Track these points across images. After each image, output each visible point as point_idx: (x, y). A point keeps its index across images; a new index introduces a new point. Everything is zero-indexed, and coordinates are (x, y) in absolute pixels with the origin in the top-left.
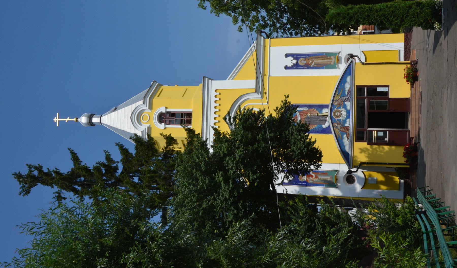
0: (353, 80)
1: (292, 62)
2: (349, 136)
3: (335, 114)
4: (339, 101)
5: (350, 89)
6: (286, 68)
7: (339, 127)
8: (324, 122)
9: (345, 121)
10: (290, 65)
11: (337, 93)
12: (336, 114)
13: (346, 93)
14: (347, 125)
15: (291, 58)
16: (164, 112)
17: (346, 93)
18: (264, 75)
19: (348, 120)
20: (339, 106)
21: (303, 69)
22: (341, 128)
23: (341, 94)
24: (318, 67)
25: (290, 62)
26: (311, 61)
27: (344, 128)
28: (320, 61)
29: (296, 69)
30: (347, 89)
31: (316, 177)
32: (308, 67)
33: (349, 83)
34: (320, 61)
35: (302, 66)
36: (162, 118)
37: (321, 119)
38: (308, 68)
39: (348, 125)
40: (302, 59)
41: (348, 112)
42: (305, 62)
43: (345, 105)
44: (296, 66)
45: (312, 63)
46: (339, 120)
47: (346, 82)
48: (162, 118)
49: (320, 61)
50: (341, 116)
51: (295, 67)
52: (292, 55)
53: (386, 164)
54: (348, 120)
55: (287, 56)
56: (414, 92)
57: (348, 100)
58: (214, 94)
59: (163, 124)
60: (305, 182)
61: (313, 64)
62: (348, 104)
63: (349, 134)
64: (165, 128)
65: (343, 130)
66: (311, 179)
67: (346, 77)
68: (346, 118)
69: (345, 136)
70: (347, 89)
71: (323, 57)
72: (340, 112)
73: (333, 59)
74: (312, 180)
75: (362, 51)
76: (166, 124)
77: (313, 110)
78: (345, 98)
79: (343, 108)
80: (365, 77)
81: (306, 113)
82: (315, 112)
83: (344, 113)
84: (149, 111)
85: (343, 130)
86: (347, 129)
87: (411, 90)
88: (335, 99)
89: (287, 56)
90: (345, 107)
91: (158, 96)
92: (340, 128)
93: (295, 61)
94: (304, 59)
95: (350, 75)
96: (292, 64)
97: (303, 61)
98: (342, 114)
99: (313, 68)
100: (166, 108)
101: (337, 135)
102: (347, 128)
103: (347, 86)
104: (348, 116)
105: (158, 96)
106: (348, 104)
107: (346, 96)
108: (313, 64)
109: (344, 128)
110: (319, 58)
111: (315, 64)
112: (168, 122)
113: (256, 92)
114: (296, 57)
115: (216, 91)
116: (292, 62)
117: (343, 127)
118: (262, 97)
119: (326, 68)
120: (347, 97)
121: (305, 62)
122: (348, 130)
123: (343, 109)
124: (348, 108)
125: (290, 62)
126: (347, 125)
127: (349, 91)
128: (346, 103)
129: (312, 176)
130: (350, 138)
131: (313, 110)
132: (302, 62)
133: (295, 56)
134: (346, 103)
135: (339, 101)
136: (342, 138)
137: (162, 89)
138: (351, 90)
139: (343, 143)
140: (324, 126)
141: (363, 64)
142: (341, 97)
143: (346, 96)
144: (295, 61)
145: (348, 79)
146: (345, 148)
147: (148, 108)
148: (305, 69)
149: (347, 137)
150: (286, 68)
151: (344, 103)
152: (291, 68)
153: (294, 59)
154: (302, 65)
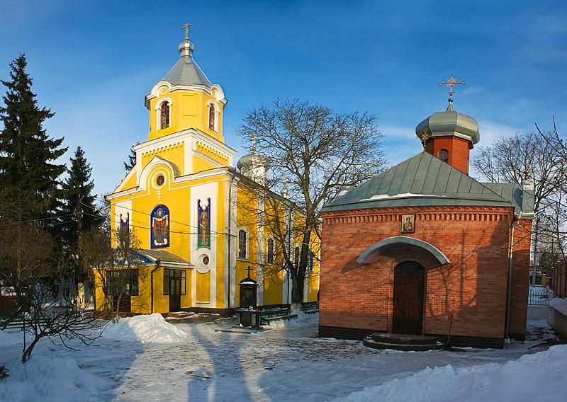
6: (199, 201)
15: (207, 203)
25: (204, 205)
32: (200, 221)
36: (165, 104)
38: (199, 221)
44: (200, 210)
52: (209, 205)
55: (209, 200)
82: (165, 233)
89: (209, 200)
93: (204, 208)
125: (204, 205)
140: (155, 241)
144: (204, 208)
150: (199, 201)
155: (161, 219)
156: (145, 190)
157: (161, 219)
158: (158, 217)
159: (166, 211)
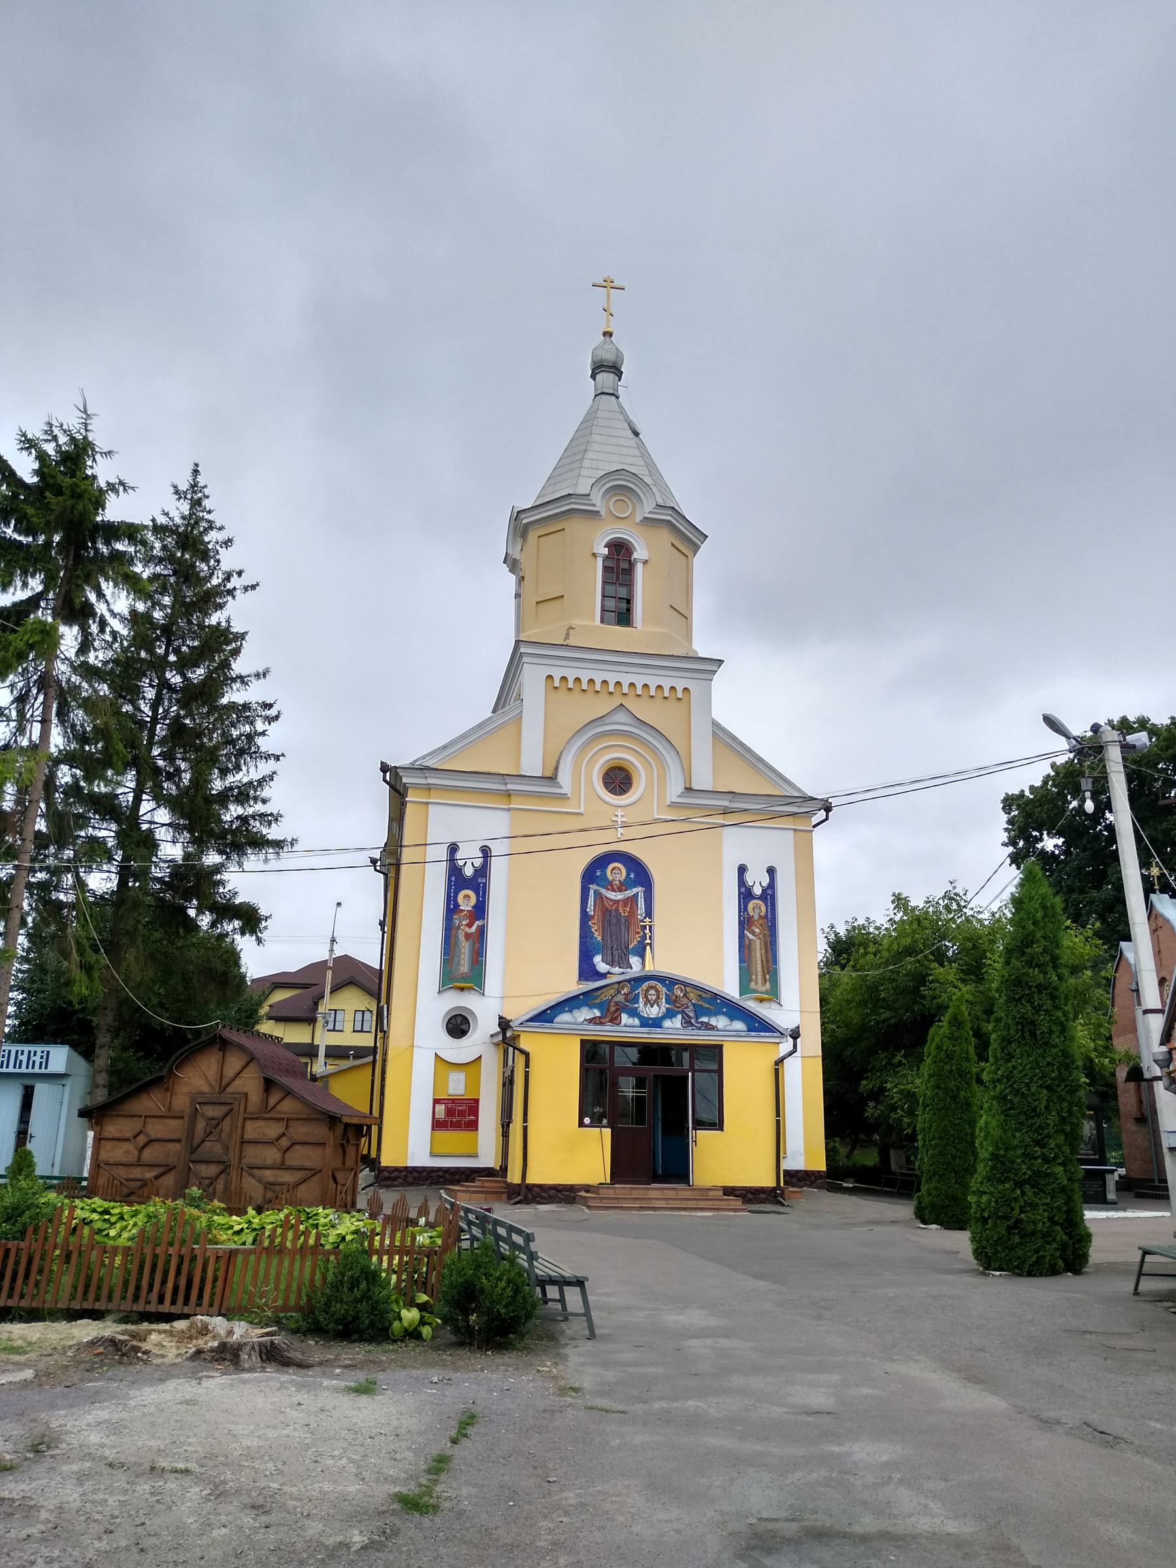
0: (737, 1034)
1: (757, 884)
2: (596, 1024)
3: (652, 987)
4: (685, 1001)
5: (713, 1028)
6: (742, 870)
7: (620, 998)
8: (609, 959)
9: (634, 1013)
10: (750, 879)
11: (703, 995)
12: (652, 992)
13: (705, 1019)
14: (625, 1018)
15: (766, 881)
16: (635, 555)
17: (705, 1019)
18: (726, 812)
21: (740, 912)
22: (617, 1004)
23: (701, 1006)
24: (744, 948)
25: (757, 880)
27: (617, 1010)
28: (758, 955)
29: (740, 893)
30: (713, 1021)
31: (468, 936)
32: (745, 923)
34: (758, 954)
35: (746, 909)
36: (620, 550)
37: (616, 953)
38: (742, 924)
39: (623, 1022)
40: (763, 908)
41: (656, 1023)
42: (756, 917)
44: (745, 894)
45: (753, 933)
46: (636, 1000)
47: (732, 1018)
48: (620, 550)
49: (758, 954)
50: (646, 1004)
51: (743, 890)
53: (525, 1120)
54: (637, 1022)
55: (771, 871)
56: (712, 1194)
57: (687, 1022)
58: (680, 685)
59: (606, 551)
60: (457, 905)
61: (751, 936)
62: (677, 1022)
63: (602, 1024)
64: (594, 554)
67: (742, 1020)
68: (641, 1018)
69: (598, 1014)
70: (713, 1021)
71: (767, 961)
73: (764, 989)
76: (606, 558)
78: (692, 1015)
79: (667, 1009)
80: (744, 1068)
81: (633, 913)
83: (654, 1012)
84: (638, 518)
85: (613, 1009)
86: (615, 1020)
87: (715, 1188)
89: (771, 871)
90: (670, 1014)
93: (758, 891)
94: (763, 914)
100: (645, 562)
102: (616, 1019)
103: (720, 1022)
104: (646, 1023)
106: (677, 1022)
108: (751, 936)
109: (617, 1010)
110: (766, 952)
111: (750, 941)
113: (689, 789)
114: (769, 895)
116: (757, 884)
117: (621, 1008)
118: (674, 805)
121: (756, 917)
123: (663, 1010)
124: (667, 1023)
125: (757, 880)
126: (625, 1018)
127: (709, 1027)
128: (680, 1016)
129: (470, 925)
130: (592, 1027)
132: (756, 908)
134: (680, 1016)
135: (685, 1001)
138: (711, 1032)
139: (578, 1008)
140: (598, 959)
144: (758, 891)
145: (739, 1025)
150: (742, 870)
151: (678, 1013)
152: (742, 882)
154: (750, 906)
155: (619, 896)
157: (619, 896)
158: (609, 885)
159: (640, 874)
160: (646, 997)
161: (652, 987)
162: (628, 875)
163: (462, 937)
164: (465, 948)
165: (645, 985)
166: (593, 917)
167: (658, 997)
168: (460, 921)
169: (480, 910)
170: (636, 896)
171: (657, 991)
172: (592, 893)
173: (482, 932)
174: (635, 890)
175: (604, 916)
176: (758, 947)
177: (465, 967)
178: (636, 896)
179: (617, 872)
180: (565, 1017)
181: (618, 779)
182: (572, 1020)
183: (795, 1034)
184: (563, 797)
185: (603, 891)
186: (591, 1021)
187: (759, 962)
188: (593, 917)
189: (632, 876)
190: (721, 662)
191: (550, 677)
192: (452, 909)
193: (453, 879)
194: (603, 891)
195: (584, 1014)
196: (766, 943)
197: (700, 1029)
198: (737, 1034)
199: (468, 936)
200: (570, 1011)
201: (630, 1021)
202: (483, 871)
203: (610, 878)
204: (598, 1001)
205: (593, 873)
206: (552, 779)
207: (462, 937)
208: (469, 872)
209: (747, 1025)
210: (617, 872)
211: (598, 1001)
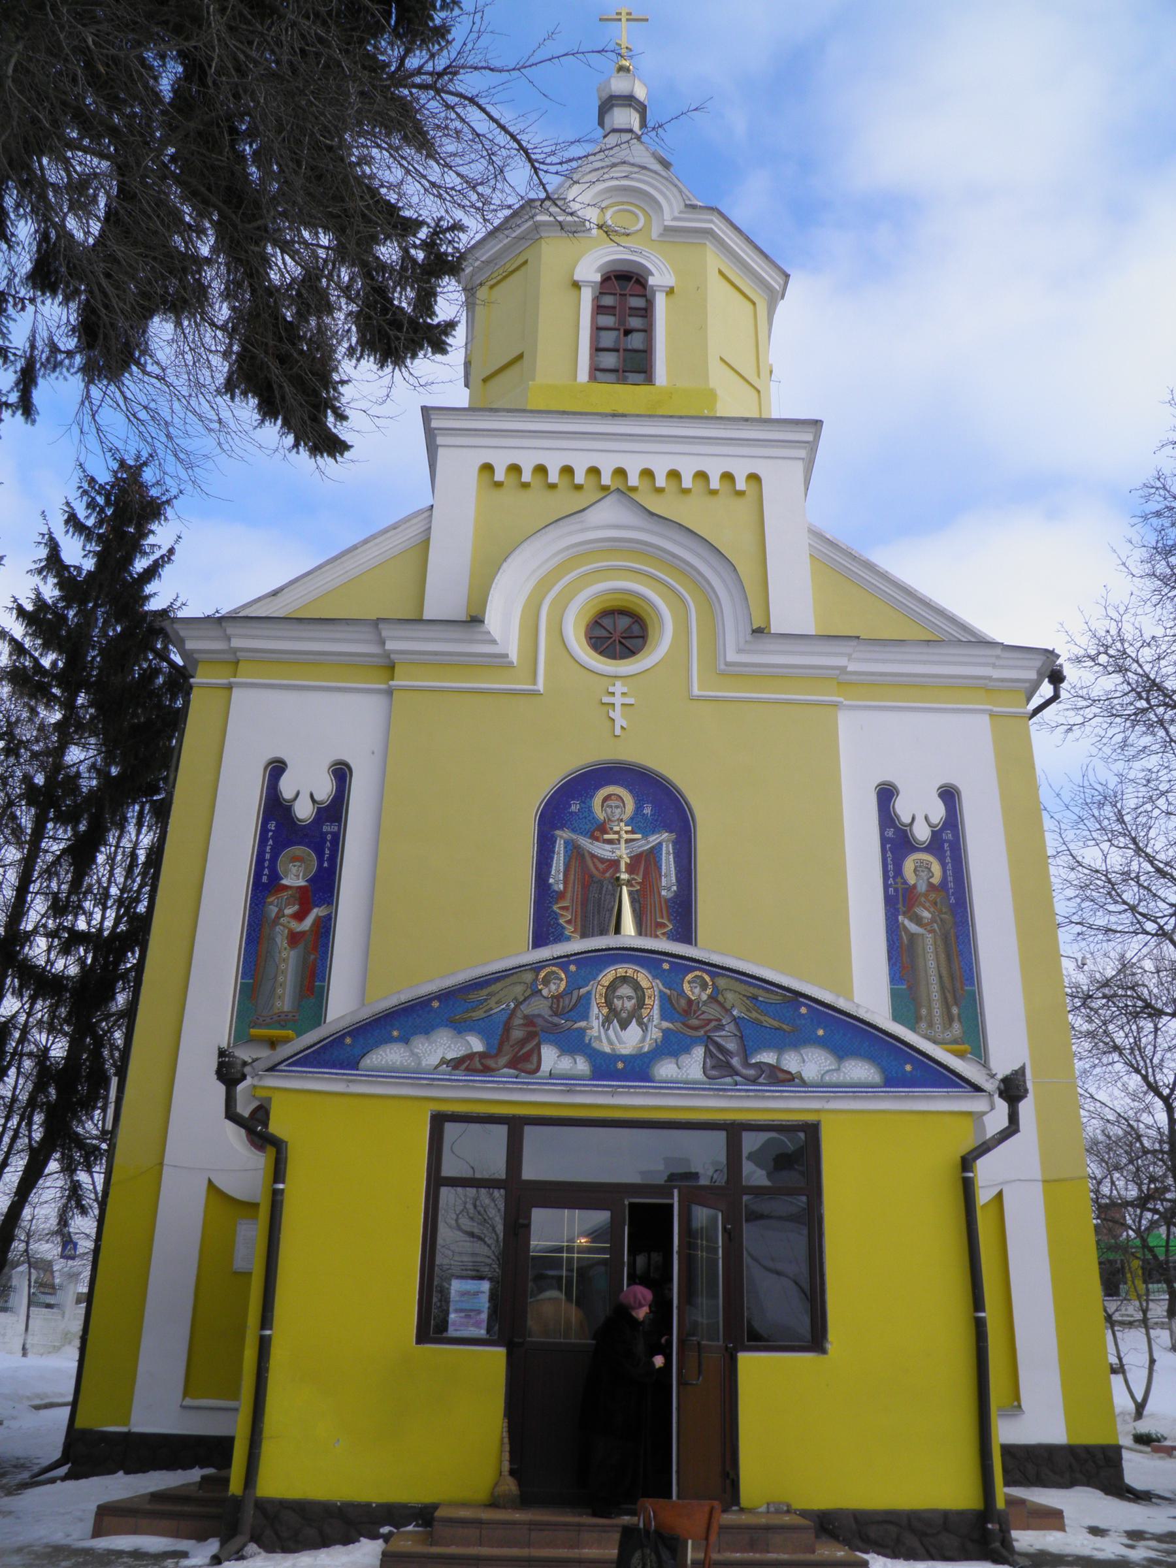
2: (471, 1070)
4: (713, 1011)
6: (886, 794)
7: (538, 1007)
9: (574, 1044)
10: (903, 808)
11: (762, 996)
12: (625, 990)
13: (768, 1057)
14: (550, 1058)
15: (938, 812)
16: (651, 281)
19: (582, 1066)
20: (678, 1009)
21: (886, 877)
22: (530, 1021)
23: (757, 1024)
25: (920, 811)
26: (926, 915)
27: (531, 1036)
28: (932, 964)
29: (884, 840)
30: (791, 1062)
31: (294, 938)
32: (898, 899)
33: (834, 1078)
35: (899, 871)
39: (546, 1067)
40: (936, 868)
41: (636, 1069)
42: (922, 887)
43: (687, 1050)
44: (896, 841)
45: (918, 920)
46: (581, 1009)
47: (841, 1053)
50: (607, 1021)
51: (890, 833)
53: (266, 1319)
54: (582, 1066)
55: (949, 795)
57: (720, 1066)
60: (275, 877)
61: (913, 928)
62: (693, 1065)
63: (486, 1070)
64: (576, 285)
65: (517, 1034)
66: (289, 911)
67: (871, 1058)
69: (476, 1044)
71: (952, 977)
72: (636, 1015)
73: (948, 1036)
74: (280, 914)
75: (1000, 1195)
77: (664, 925)
78: (731, 1046)
79: (666, 1032)
83: (630, 1040)
85: (517, 1034)
86: (524, 1061)
88: (722, 982)
89: (949, 795)
90: (672, 1046)
91: (720, 272)
92: (527, 1009)
93: (922, 833)
94: (936, 880)
95: (890, 1082)
96: (906, 819)
97: (924, 875)
98: (624, 1025)
99: (893, 929)
100: (670, 291)
101: (485, 992)
102: (527, 1057)
103: (810, 1063)
105: (720, 272)
106: (693, 1065)
107: (746, 1055)
108: (913, 928)
109: (531, 1036)
111: (912, 937)
112: (608, 301)
114: (948, 841)
115: (754, 478)
119: (895, 995)
120: (735, 1062)
121: (922, 887)
122: (512, 1064)
123: (655, 1034)
124: (666, 1069)
125: (920, 811)
126: (550, 1058)
128: (699, 1052)
129: (300, 916)
131: (664, 925)
132: (923, 870)
133: (948, 835)
134: (699, 1052)
135: (713, 1011)
136: (460, 1027)
137: (754, 304)
139: (427, 1030)
141: (967, 1163)
142: (735, 1020)
143: (746, 1055)
144: (922, 833)
145: (860, 1071)
146: (390, 1040)
147: (666, 223)
148: (886, 887)
149: (470, 1056)
150: (886, 794)
151: (695, 1041)
153: (936, 835)
154: (909, 865)
156: (514, 657)
159: (664, 805)
160: (609, 1003)
161: (624, 979)
162: (638, 809)
163: (281, 941)
164: (287, 963)
165: (608, 975)
166: (561, 895)
167: (641, 1004)
168: (282, 909)
169: (324, 886)
170: (655, 852)
171: (637, 987)
172: (560, 847)
173: (324, 931)
174: (654, 839)
175: (586, 887)
176: (930, 948)
177: (285, 998)
178: (655, 852)
179: (616, 805)
180: (390, 1055)
181: (620, 631)
182: (410, 1062)
183: (1012, 1090)
184: (499, 662)
185: (585, 842)
186: (456, 1064)
187: (934, 980)
188: (561, 895)
189: (648, 810)
190: (817, 424)
191: (488, 468)
192: (264, 883)
193: (272, 826)
194: (585, 842)
195: (440, 1047)
196: (946, 938)
197: (754, 1081)
198: (856, 1089)
199: (294, 938)
200: (405, 1040)
201: (565, 1064)
202: (334, 811)
203: (600, 814)
204: (479, 1014)
205: (564, 807)
206: (476, 620)
207: (281, 941)
208: (304, 811)
209: (883, 1070)
210: (616, 805)
211: (479, 1014)
